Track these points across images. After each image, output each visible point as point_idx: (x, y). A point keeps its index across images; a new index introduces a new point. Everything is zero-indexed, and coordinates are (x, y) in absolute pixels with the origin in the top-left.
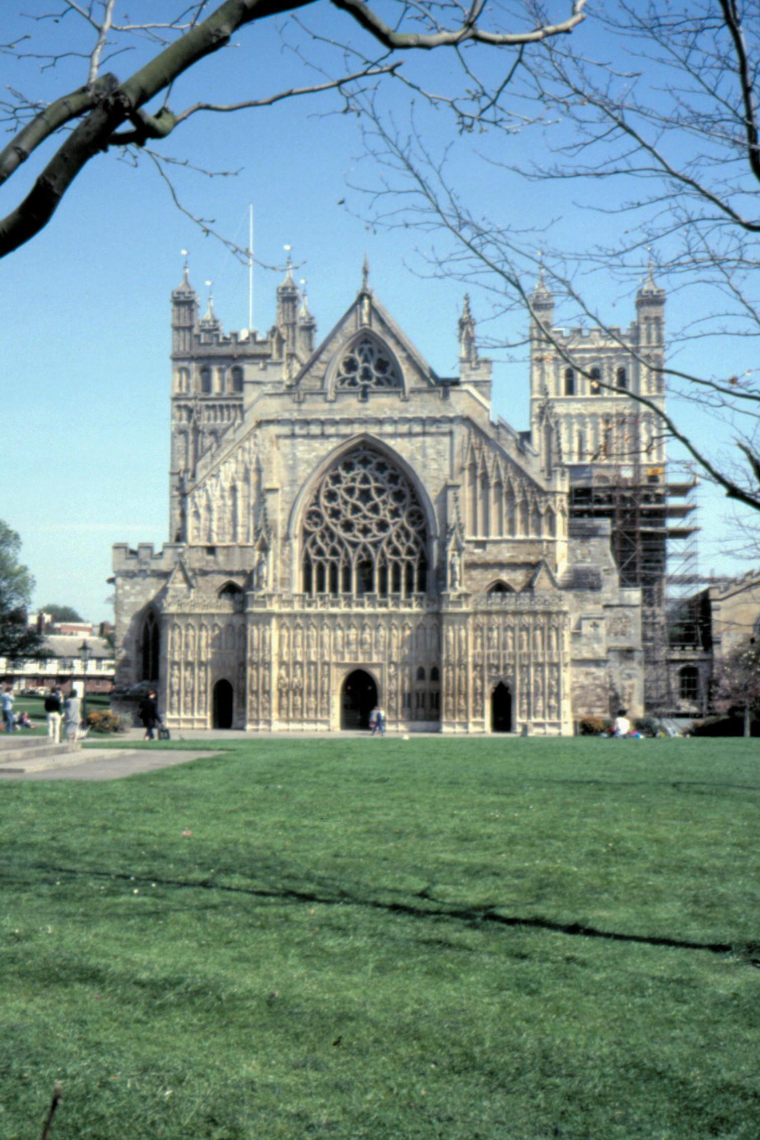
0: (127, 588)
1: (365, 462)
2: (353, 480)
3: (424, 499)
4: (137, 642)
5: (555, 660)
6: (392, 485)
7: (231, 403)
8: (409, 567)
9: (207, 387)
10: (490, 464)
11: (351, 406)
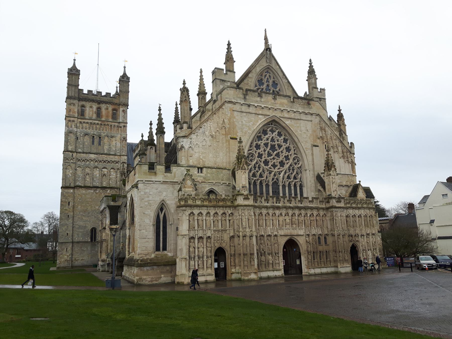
0: (147, 191)
1: (272, 131)
2: (267, 139)
3: (302, 151)
4: (153, 225)
5: (374, 232)
6: (285, 144)
7: (97, 122)
8: (295, 185)
9: (82, 114)
10: (329, 138)
11: (268, 100)
